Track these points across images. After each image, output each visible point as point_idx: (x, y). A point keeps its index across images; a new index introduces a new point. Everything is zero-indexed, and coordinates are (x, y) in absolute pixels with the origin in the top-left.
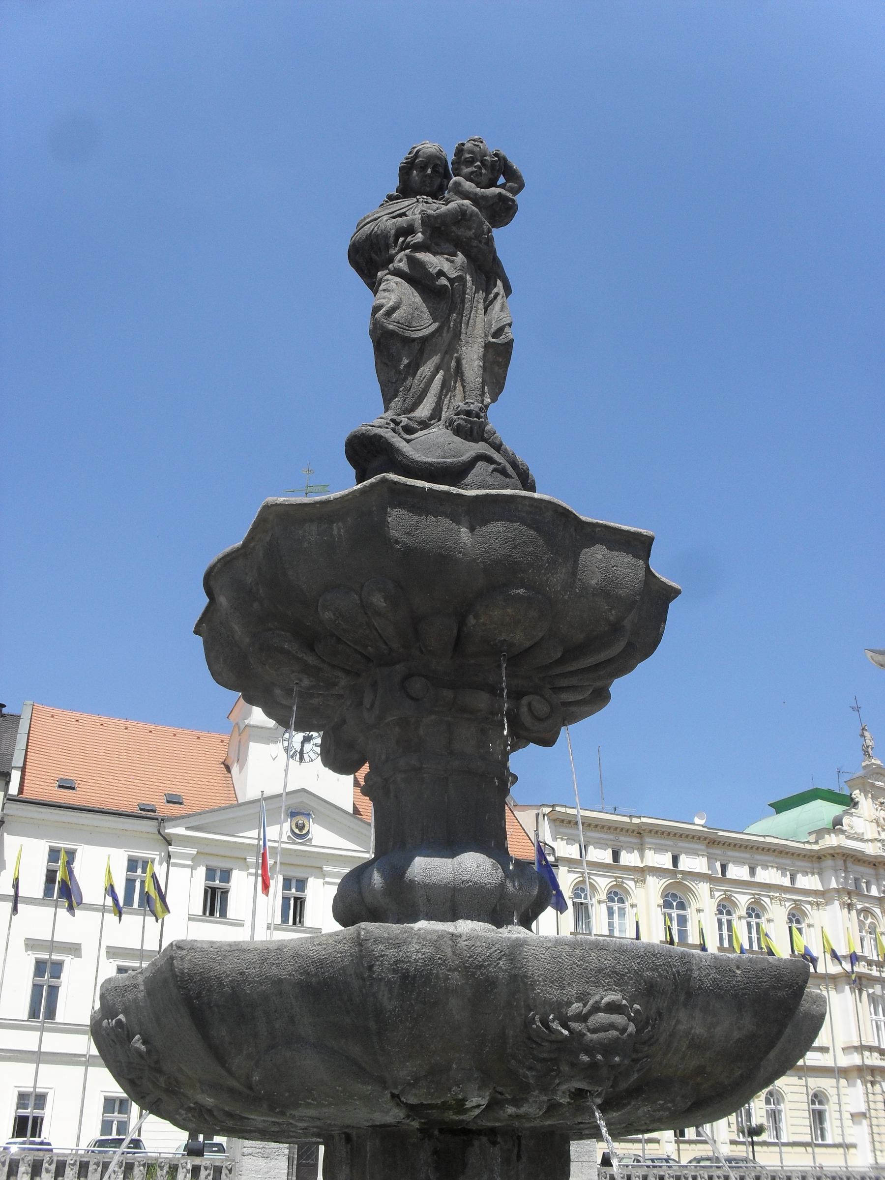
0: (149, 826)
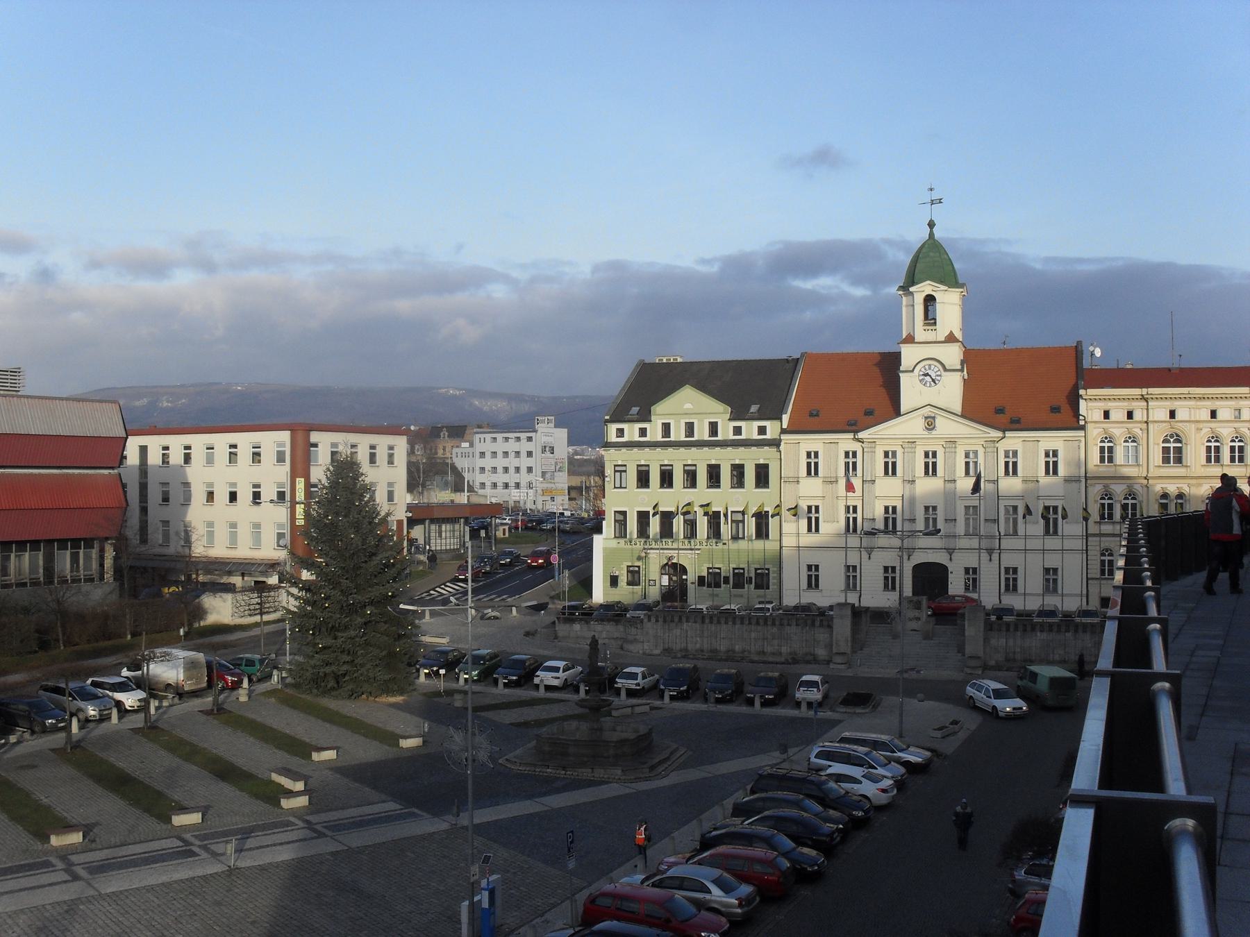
0: (851, 436)
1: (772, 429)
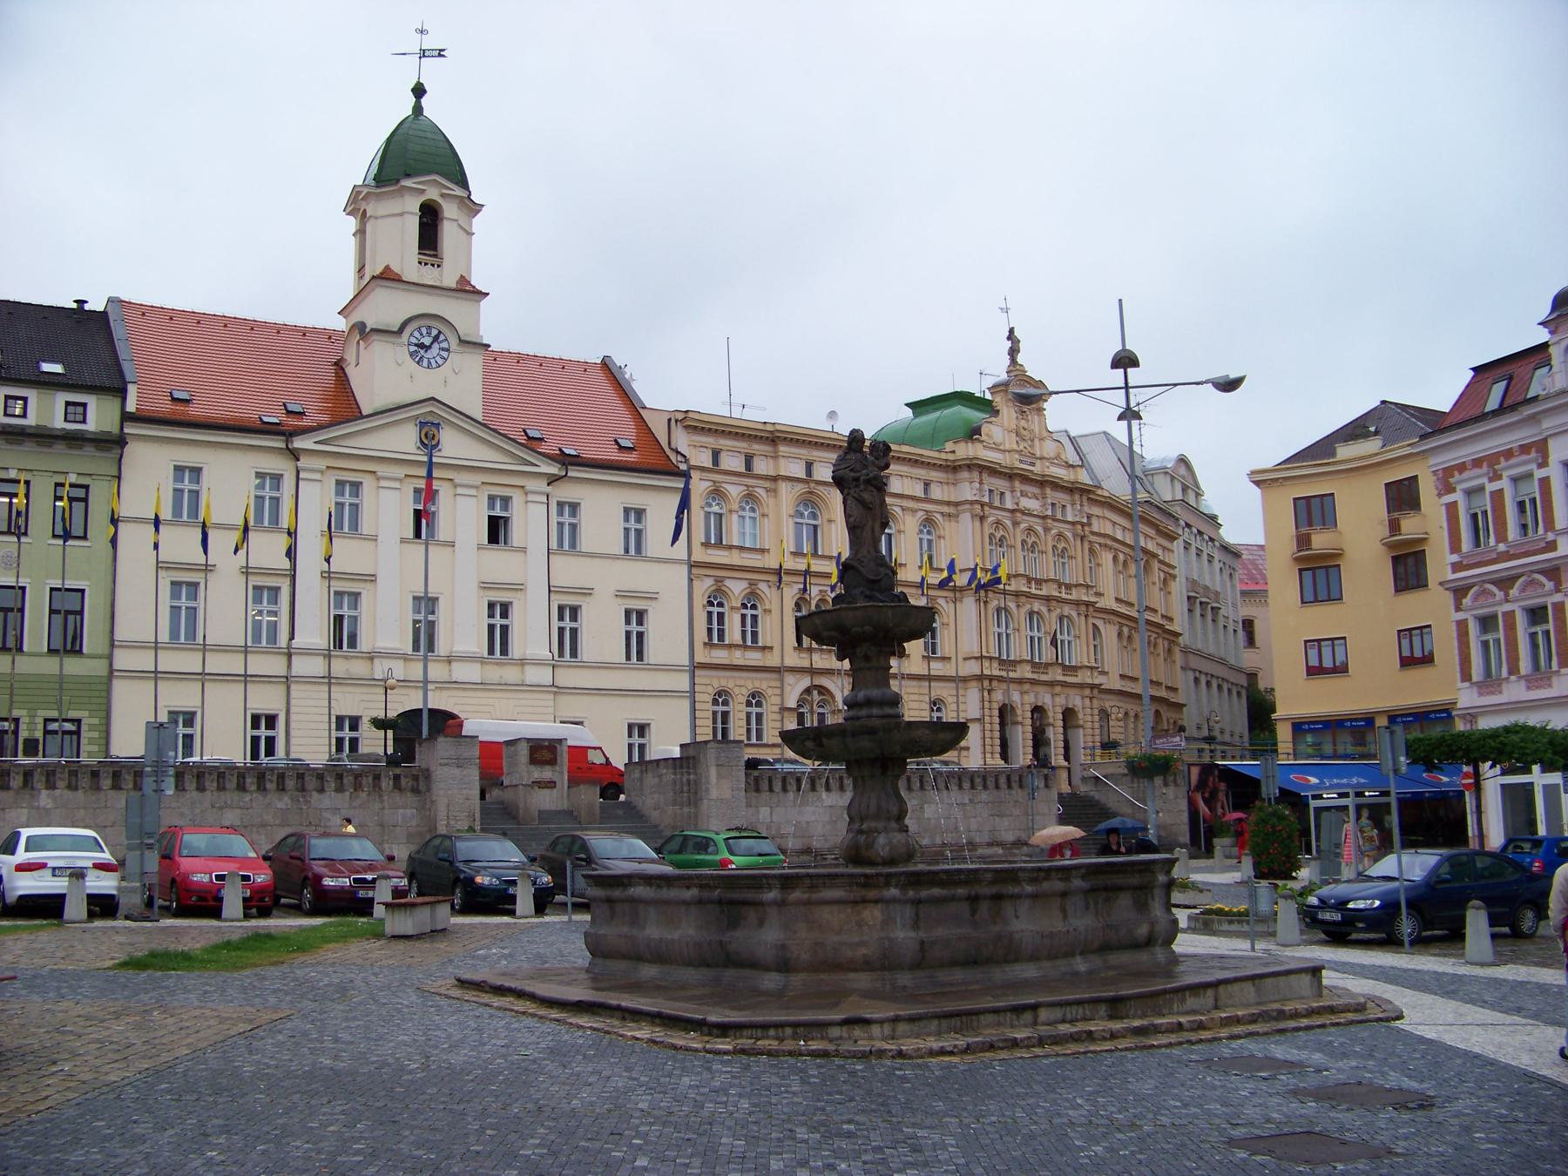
0: (278, 443)
1: (100, 415)
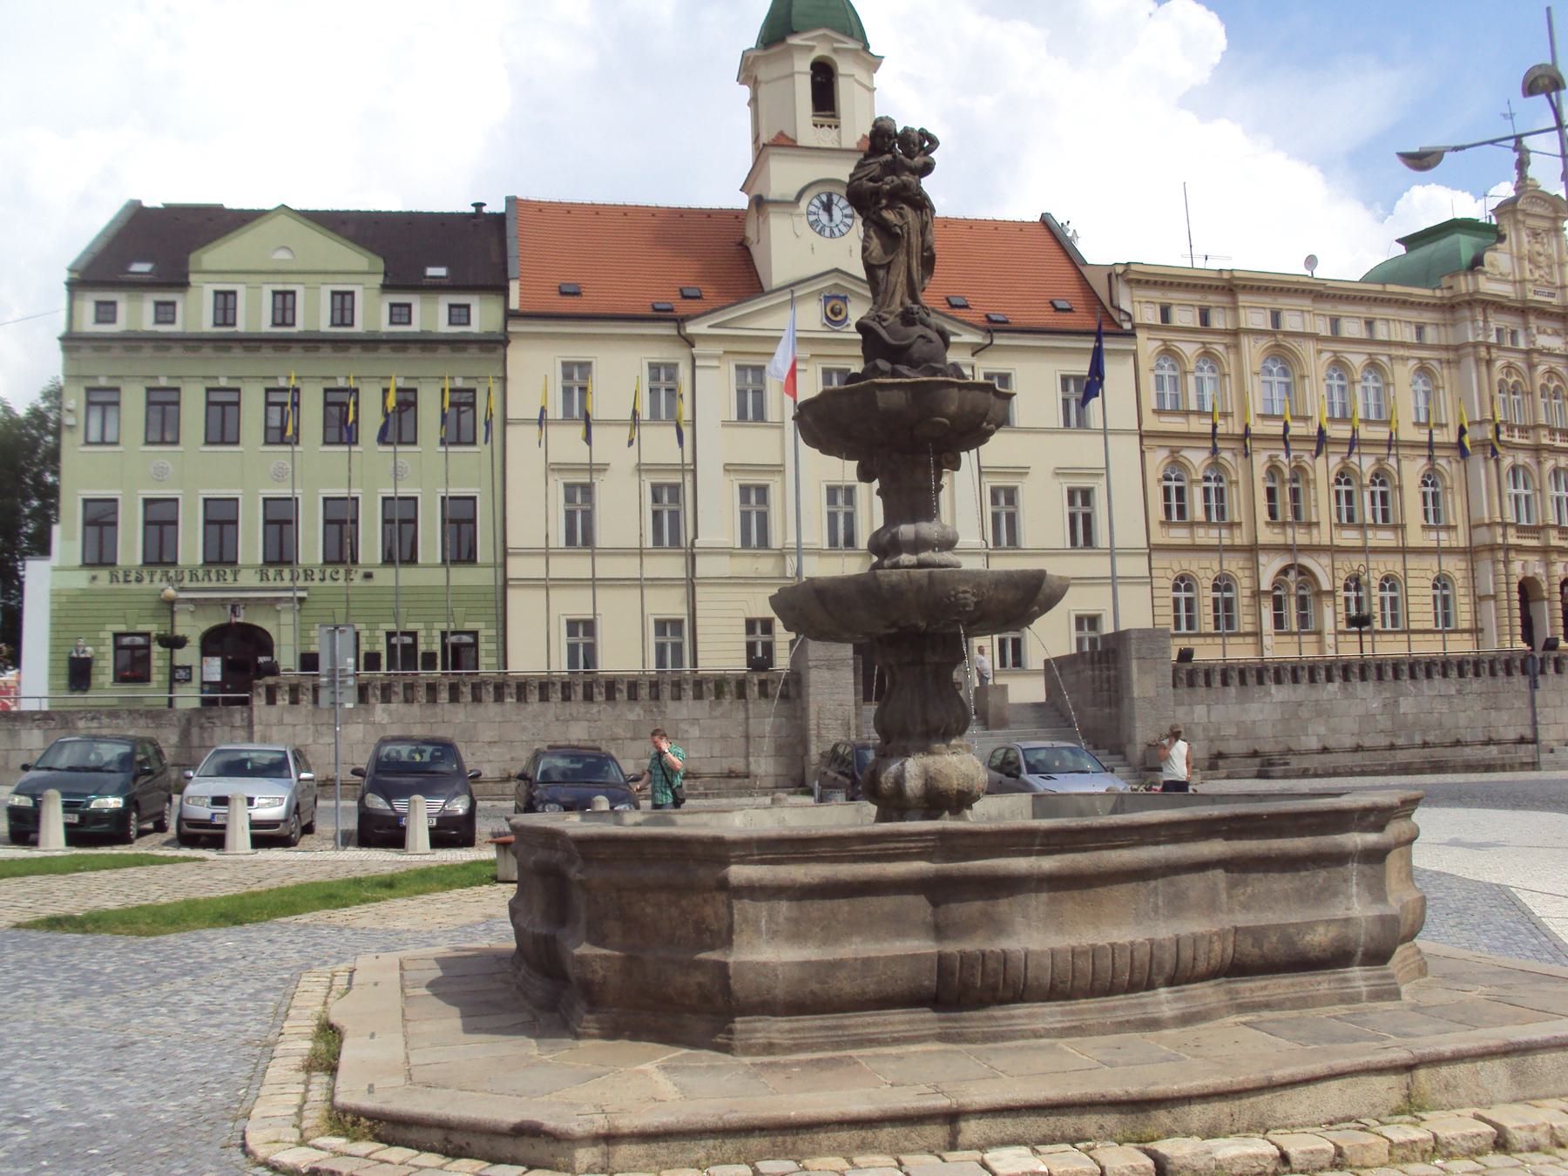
0: (667, 330)
1: (483, 315)
